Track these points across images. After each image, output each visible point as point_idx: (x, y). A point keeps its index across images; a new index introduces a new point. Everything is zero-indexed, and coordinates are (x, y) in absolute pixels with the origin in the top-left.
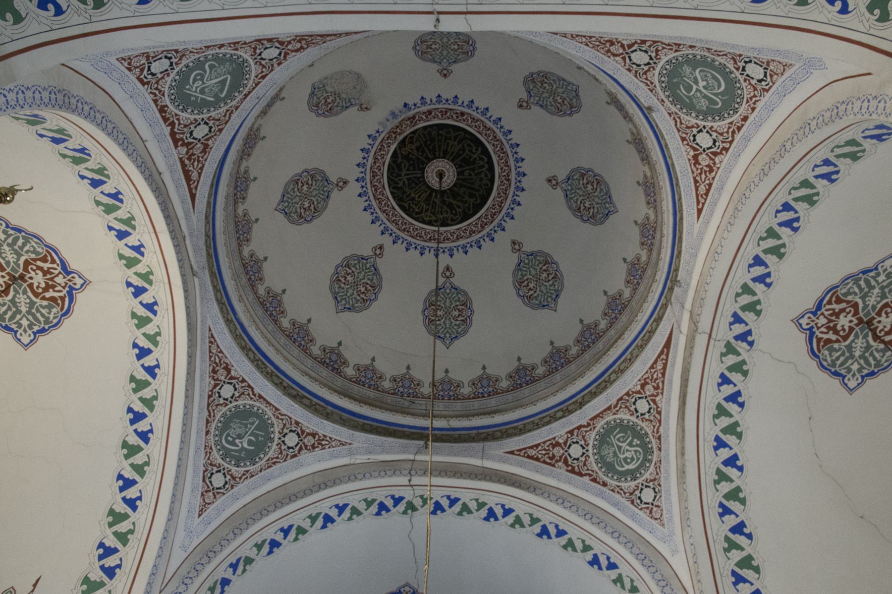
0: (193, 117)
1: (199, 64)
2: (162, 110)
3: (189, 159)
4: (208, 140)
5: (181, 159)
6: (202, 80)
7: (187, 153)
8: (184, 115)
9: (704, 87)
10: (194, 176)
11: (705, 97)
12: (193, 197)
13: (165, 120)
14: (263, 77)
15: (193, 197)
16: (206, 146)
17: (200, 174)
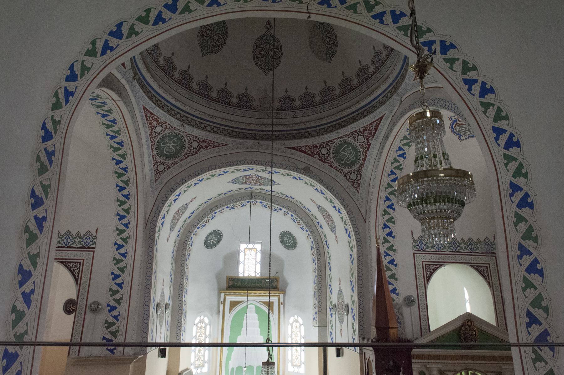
0: (359, 147)
1: (345, 165)
2: (364, 160)
3: (370, 134)
4: (361, 133)
5: (373, 137)
6: (348, 158)
7: (370, 137)
8: (361, 151)
10: (375, 125)
11: (167, 143)
12: (381, 118)
13: (366, 156)
14: (331, 141)
15: (381, 118)
16: (364, 130)
17: (373, 123)
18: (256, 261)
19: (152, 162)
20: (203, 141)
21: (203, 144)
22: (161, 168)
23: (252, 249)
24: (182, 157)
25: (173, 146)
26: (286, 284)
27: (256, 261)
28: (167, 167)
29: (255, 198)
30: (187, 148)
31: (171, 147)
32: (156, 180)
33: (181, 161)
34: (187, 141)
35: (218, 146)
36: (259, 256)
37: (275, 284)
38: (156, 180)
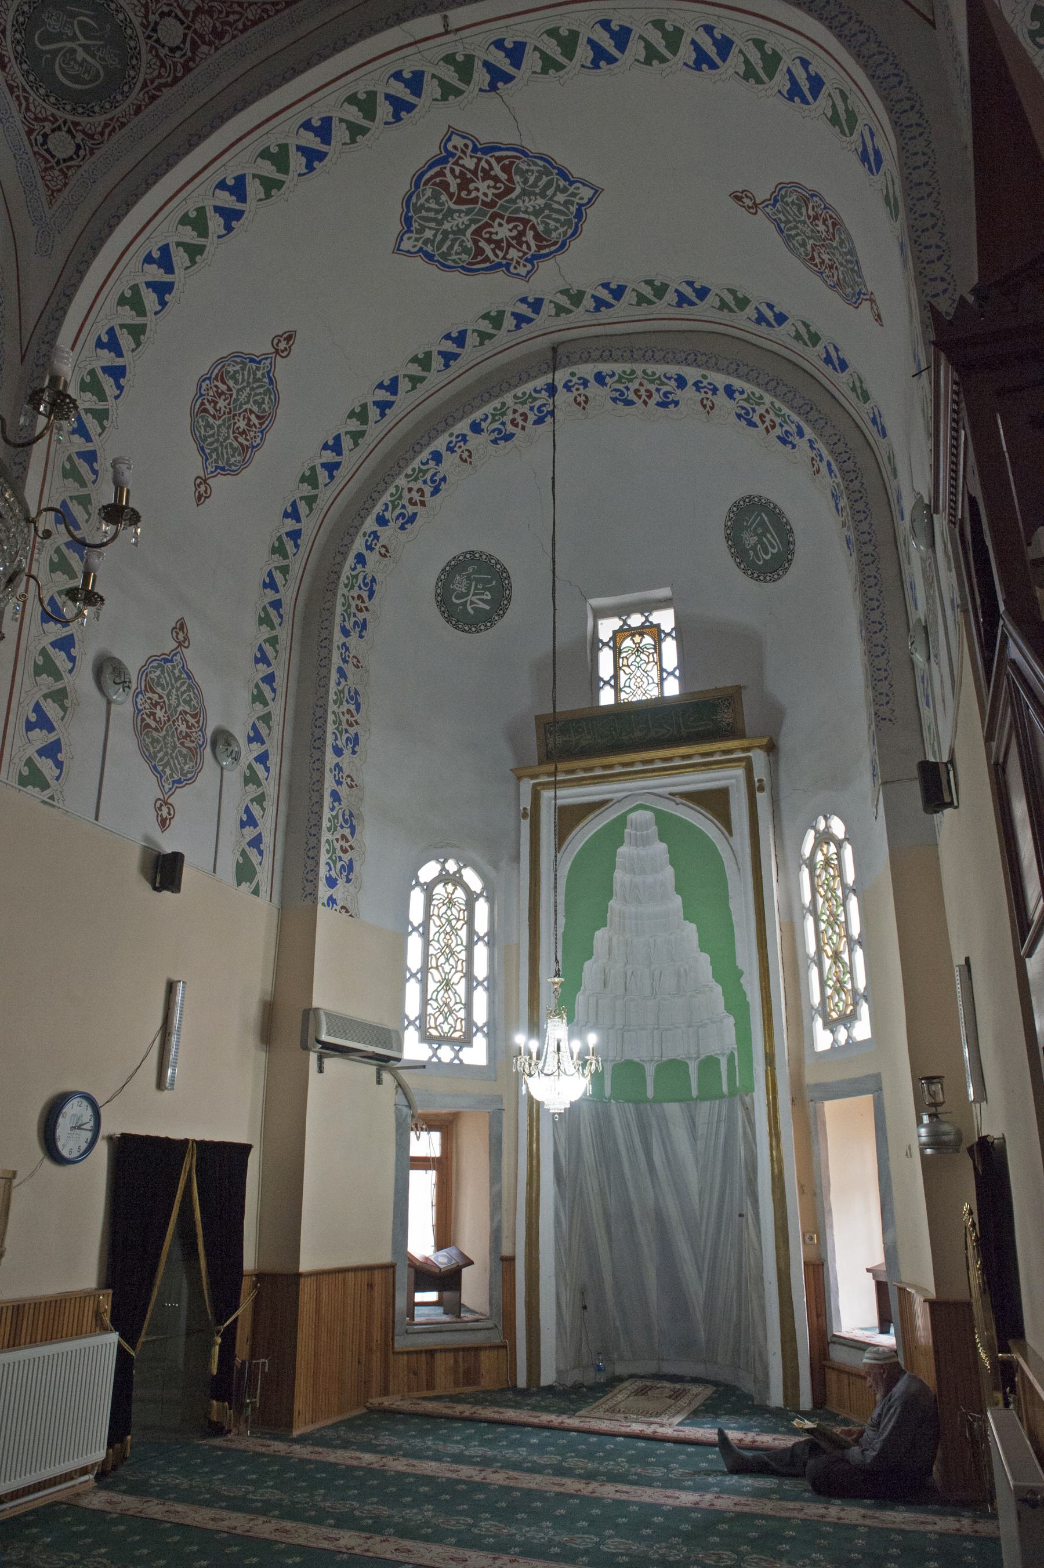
9: (73, 51)
11: (59, 37)
18: (662, 670)
19: (18, 117)
20: (199, 10)
21: (204, 24)
22: (62, 145)
23: (641, 631)
24: (136, 95)
25: (85, 47)
26: (775, 715)
27: (662, 670)
28: (89, 143)
29: (571, 362)
30: (146, 57)
31: (81, 54)
32: (53, 193)
33: (138, 110)
34: (137, 22)
35: (261, 19)
36: (670, 648)
37: (725, 717)
38: (53, 193)
